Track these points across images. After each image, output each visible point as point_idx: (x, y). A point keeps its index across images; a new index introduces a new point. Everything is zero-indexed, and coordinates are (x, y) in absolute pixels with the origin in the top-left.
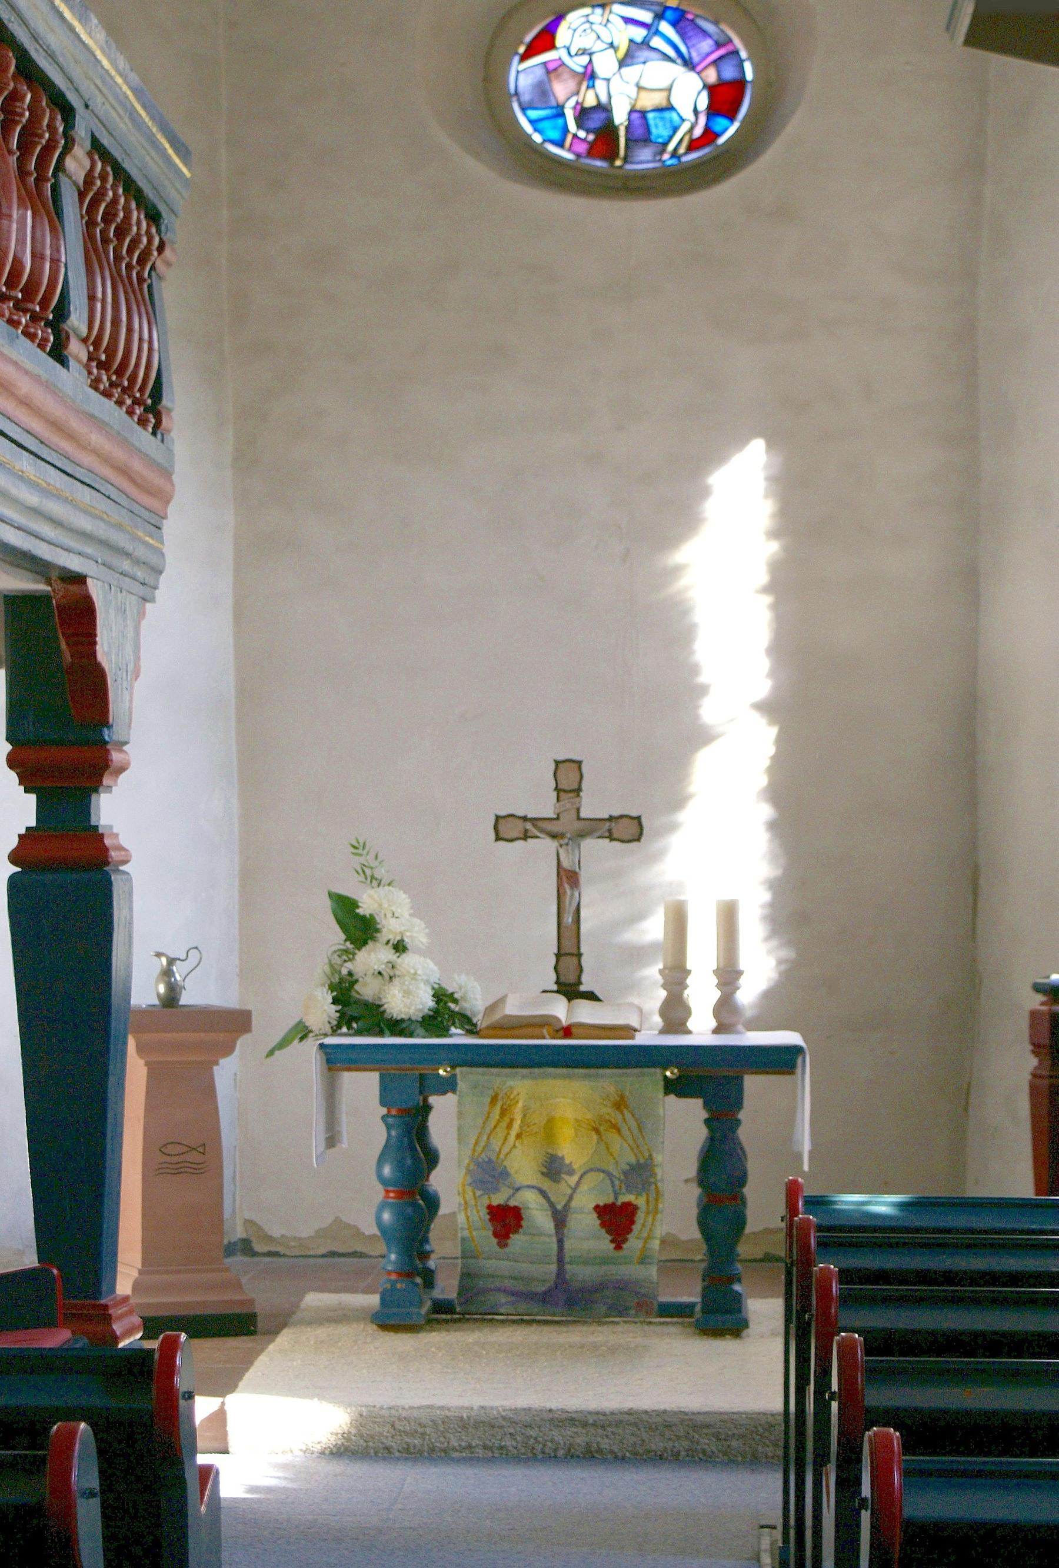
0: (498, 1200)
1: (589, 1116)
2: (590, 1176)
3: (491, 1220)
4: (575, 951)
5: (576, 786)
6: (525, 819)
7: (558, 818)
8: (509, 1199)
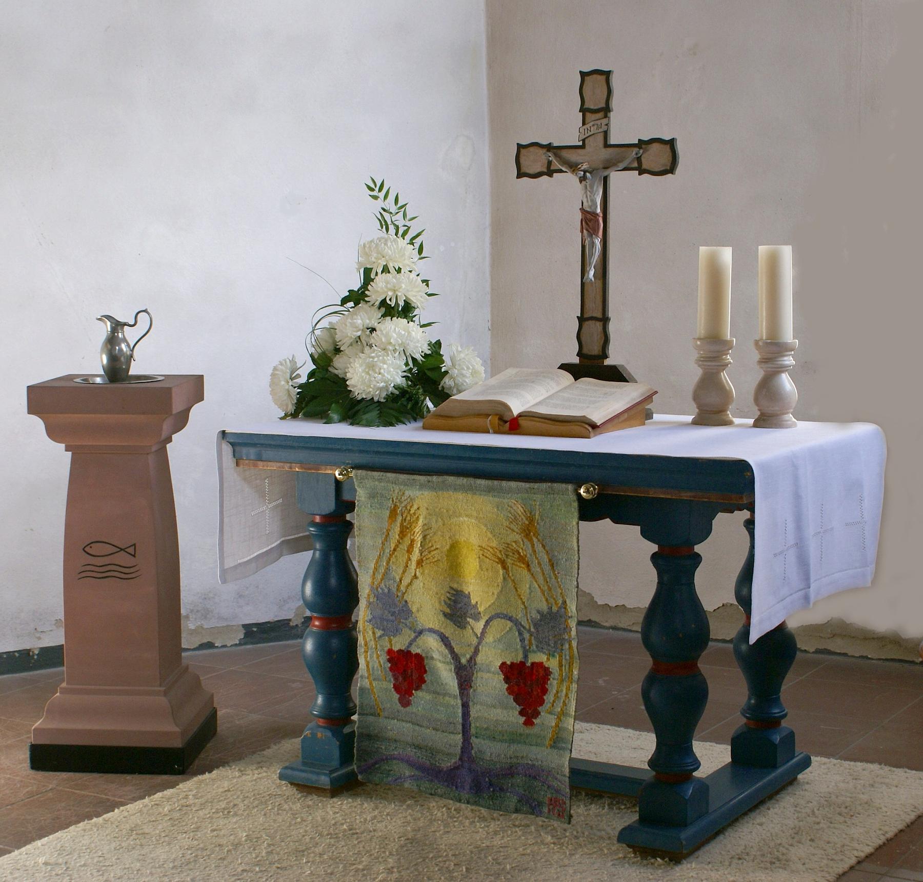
0: (399, 644)
1: (494, 544)
2: (496, 623)
3: (391, 669)
4: (599, 315)
5: (603, 105)
6: (549, 147)
7: (583, 147)
8: (410, 644)
